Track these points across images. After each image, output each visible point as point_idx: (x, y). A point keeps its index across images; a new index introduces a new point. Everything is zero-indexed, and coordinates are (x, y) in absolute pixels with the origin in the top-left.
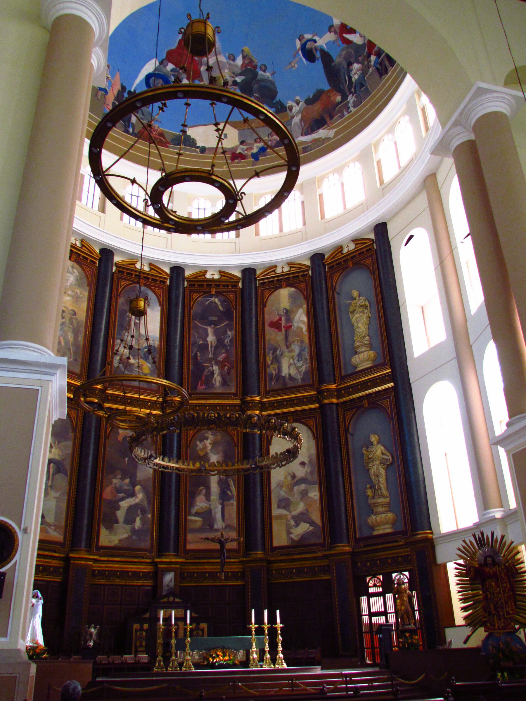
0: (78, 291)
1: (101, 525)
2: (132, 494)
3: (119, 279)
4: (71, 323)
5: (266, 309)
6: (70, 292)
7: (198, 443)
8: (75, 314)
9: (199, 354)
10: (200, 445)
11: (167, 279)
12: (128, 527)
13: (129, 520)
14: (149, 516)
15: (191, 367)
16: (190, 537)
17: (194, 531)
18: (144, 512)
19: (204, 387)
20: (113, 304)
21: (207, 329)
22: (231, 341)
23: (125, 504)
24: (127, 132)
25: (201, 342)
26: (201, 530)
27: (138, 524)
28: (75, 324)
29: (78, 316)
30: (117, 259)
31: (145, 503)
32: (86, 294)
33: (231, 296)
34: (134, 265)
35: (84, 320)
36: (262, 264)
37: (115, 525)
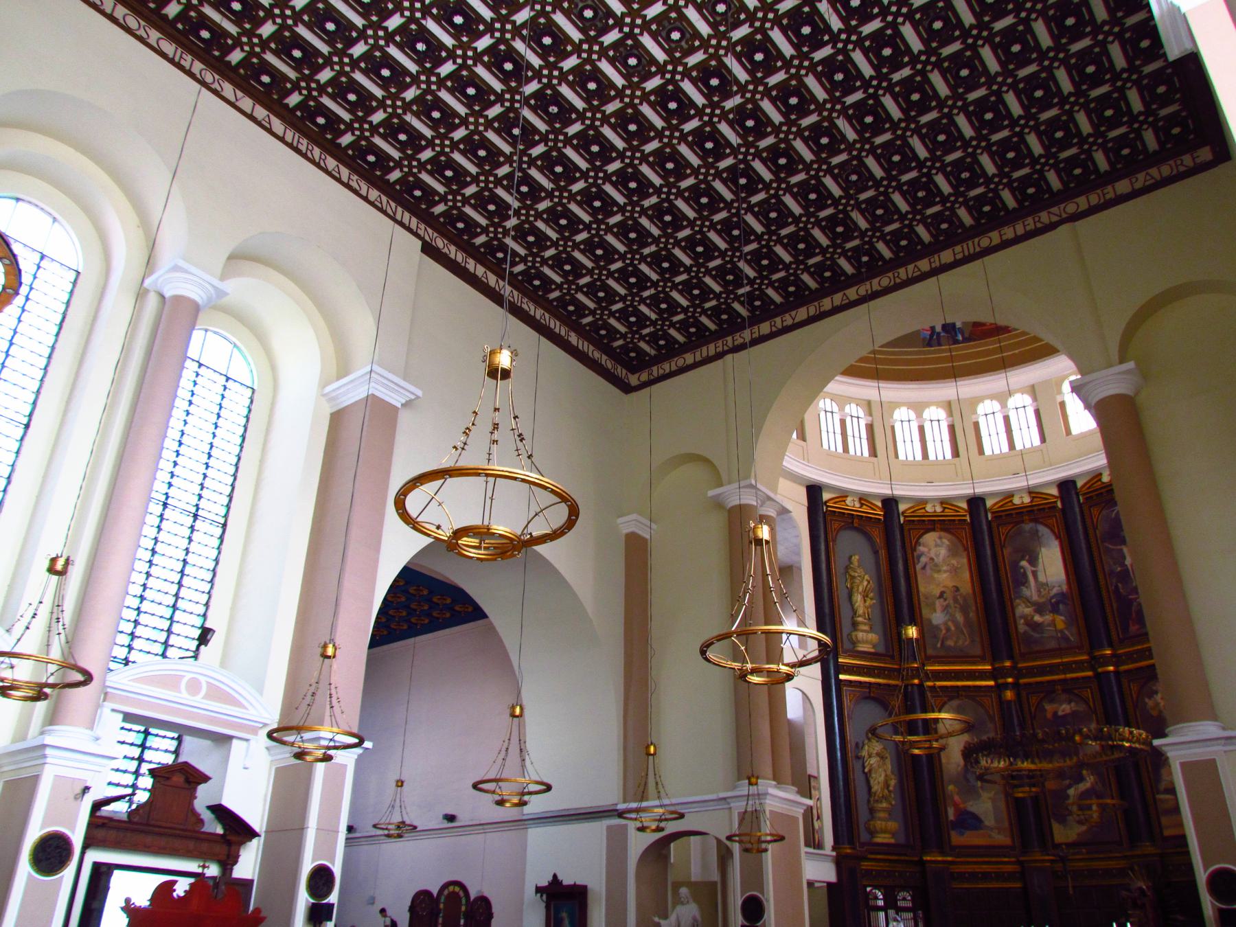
0: (954, 562)
2: (1081, 779)
3: (998, 526)
6: (945, 568)
7: (1147, 700)
8: (957, 589)
9: (1120, 585)
10: (1150, 703)
11: (1055, 502)
15: (1115, 605)
19: (1137, 627)
21: (1121, 550)
24: (956, 342)
25: (1119, 569)
28: (961, 601)
29: (962, 590)
30: (989, 503)
32: (965, 561)
34: (1011, 501)
35: (970, 591)
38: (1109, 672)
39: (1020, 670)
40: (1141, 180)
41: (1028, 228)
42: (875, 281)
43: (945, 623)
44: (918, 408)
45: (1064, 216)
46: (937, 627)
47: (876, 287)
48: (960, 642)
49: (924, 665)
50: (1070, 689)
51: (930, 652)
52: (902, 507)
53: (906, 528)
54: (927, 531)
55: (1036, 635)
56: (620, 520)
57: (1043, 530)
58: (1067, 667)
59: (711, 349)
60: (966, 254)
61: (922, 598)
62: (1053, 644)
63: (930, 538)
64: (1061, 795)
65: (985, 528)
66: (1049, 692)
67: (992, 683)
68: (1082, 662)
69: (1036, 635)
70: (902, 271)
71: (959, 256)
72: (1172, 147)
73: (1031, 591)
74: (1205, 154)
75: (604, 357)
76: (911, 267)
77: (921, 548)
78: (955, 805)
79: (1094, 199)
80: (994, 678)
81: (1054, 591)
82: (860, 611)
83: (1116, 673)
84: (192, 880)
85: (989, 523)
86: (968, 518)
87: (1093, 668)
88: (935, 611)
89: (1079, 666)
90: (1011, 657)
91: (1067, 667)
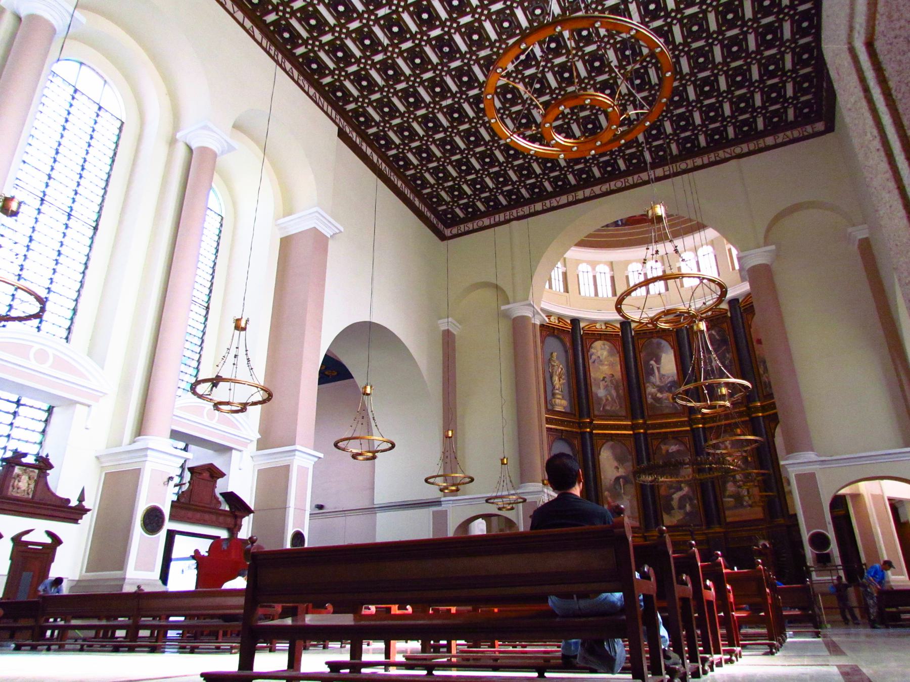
0: (611, 359)
1: (663, 513)
2: (680, 489)
3: (638, 339)
4: (612, 383)
5: (752, 330)
8: (613, 376)
12: (682, 511)
13: (681, 507)
14: (695, 502)
16: (727, 513)
17: (729, 509)
18: (691, 499)
20: (638, 358)
22: (730, 362)
23: (676, 496)
26: (735, 507)
27: (688, 508)
31: (691, 494)
32: (618, 359)
33: (725, 325)
35: (620, 377)
36: (741, 294)
37: (673, 512)
38: (699, 428)
39: (649, 424)
40: (781, 138)
41: (711, 160)
42: (612, 183)
43: (606, 396)
44: (593, 264)
45: (733, 154)
46: (601, 399)
47: (613, 187)
48: (613, 408)
49: (593, 420)
50: (676, 436)
51: (596, 413)
52: (582, 325)
53: (584, 338)
54: (597, 340)
55: (658, 405)
56: (440, 321)
57: (664, 343)
58: (675, 425)
59: (501, 217)
60: (672, 172)
61: (592, 380)
62: (667, 411)
63: (598, 344)
64: (669, 498)
65: (630, 339)
66: (664, 438)
67: (631, 432)
68: (684, 421)
69: (658, 405)
70: (630, 178)
71: (667, 173)
72: (802, 120)
73: (656, 379)
74: (820, 126)
75: (432, 216)
76: (636, 177)
77: (593, 350)
78: (609, 503)
79: (752, 146)
80: (632, 429)
81: (670, 379)
82: (557, 387)
83: (703, 428)
84: (211, 541)
85: (632, 337)
86: (620, 333)
87: (690, 426)
88: (600, 388)
89: (683, 424)
90: (643, 418)
91: (675, 425)
